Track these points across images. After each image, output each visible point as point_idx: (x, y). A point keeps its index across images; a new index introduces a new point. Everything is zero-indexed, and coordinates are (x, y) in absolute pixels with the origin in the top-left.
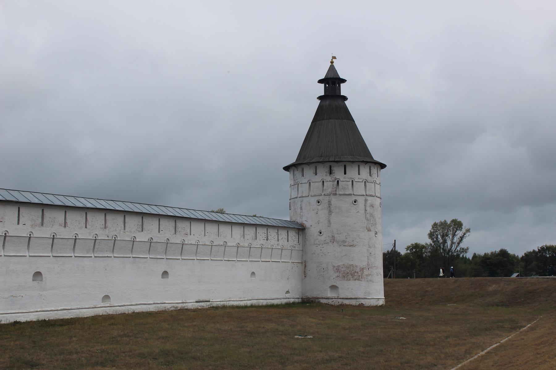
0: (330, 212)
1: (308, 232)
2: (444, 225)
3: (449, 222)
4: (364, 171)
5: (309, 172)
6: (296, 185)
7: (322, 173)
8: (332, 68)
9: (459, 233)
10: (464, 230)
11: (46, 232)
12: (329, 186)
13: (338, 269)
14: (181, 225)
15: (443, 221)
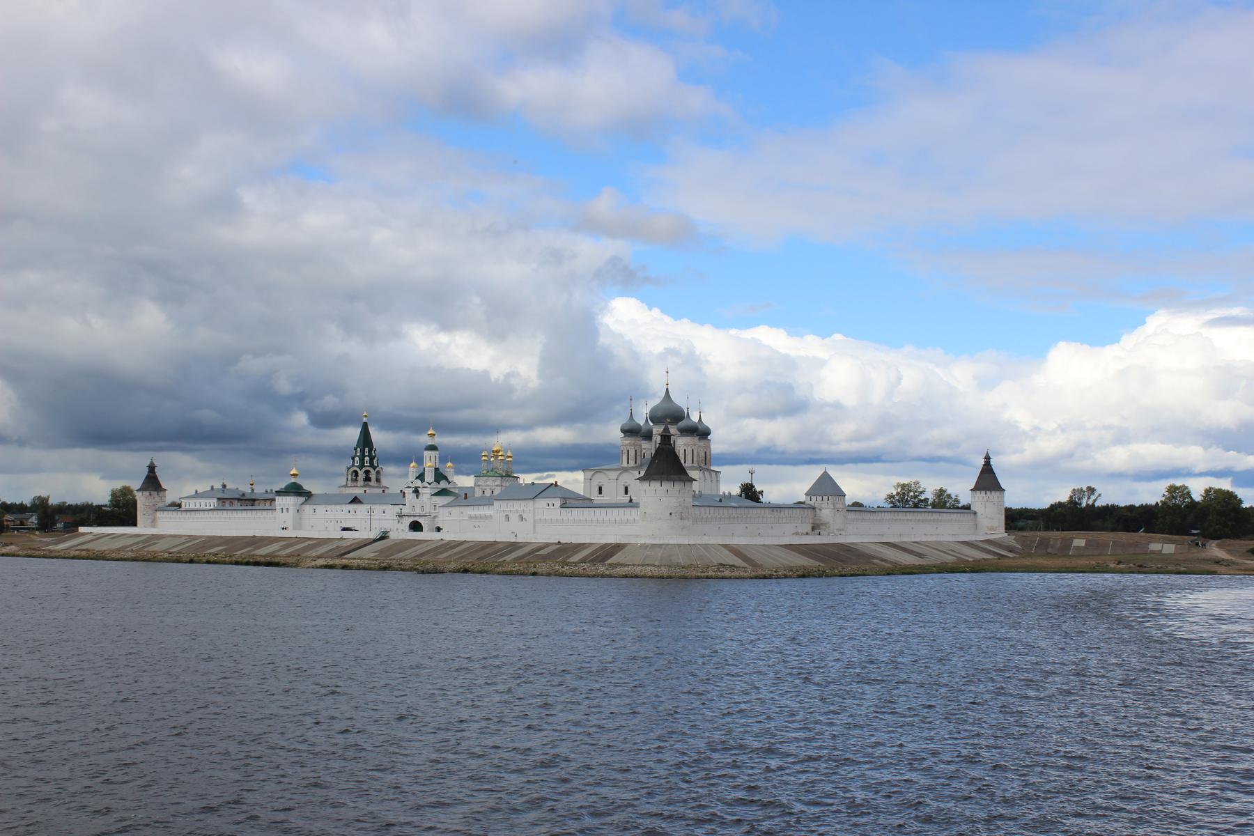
0: (985, 507)
1: (979, 514)
2: (1081, 490)
3: (1085, 489)
4: (998, 493)
5: (978, 492)
6: (973, 497)
7: (983, 492)
8: (987, 454)
9: (1093, 497)
10: (1096, 495)
11: (914, 518)
12: (985, 498)
13: (987, 527)
14: (941, 514)
15: (1080, 487)
